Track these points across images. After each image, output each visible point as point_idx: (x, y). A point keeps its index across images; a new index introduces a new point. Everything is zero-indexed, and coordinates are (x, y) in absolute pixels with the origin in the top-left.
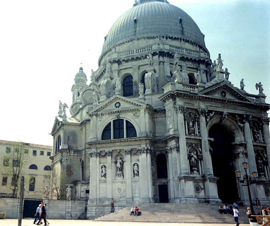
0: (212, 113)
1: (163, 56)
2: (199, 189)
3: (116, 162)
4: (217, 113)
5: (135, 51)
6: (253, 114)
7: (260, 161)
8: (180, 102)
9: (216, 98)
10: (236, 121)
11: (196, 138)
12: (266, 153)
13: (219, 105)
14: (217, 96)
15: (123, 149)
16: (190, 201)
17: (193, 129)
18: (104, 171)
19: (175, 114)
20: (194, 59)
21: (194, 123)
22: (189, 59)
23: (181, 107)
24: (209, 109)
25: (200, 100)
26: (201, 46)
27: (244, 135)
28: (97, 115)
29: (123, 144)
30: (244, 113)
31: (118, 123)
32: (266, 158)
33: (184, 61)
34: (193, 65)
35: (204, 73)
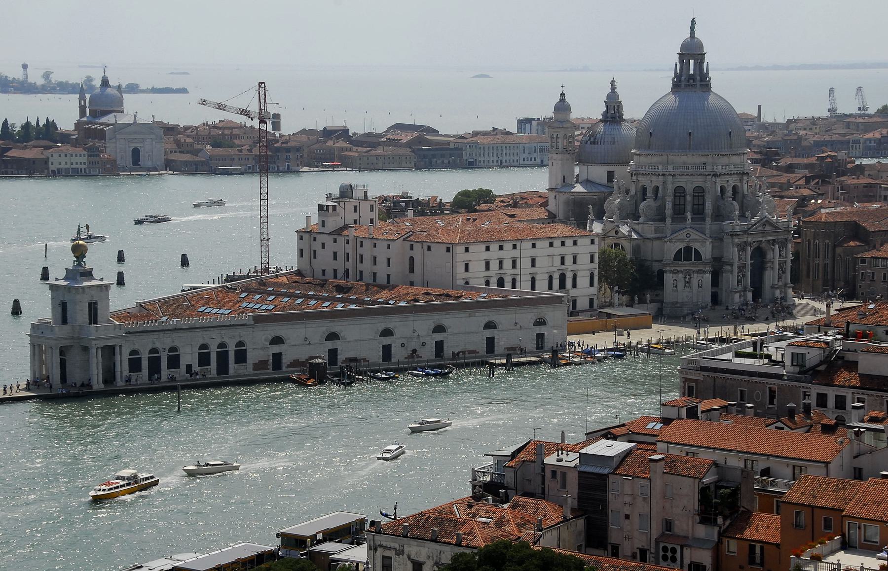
1: (715, 177)
3: (685, 278)
5: (690, 167)
7: (780, 272)
8: (737, 240)
10: (770, 244)
12: (786, 265)
13: (761, 235)
14: (760, 228)
15: (692, 270)
18: (675, 283)
19: (732, 249)
21: (742, 252)
25: (748, 234)
27: (773, 254)
28: (670, 241)
29: (692, 266)
31: (688, 250)
32: (785, 269)
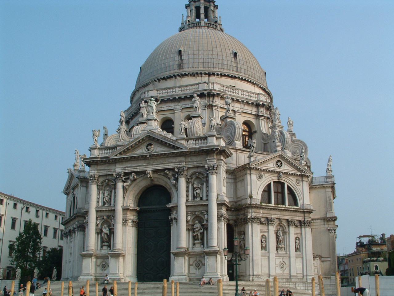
0: (131, 175)
2: (105, 266)
4: (137, 173)
6: (195, 163)
9: (132, 156)
10: (169, 179)
11: (108, 209)
14: (142, 151)
16: (83, 279)
17: (107, 198)
20: (190, 96)
22: (183, 98)
23: (91, 176)
24: (127, 171)
26: (210, 73)
30: (176, 166)
32: (207, 221)
33: (179, 102)
34: (191, 104)
35: (205, 110)
